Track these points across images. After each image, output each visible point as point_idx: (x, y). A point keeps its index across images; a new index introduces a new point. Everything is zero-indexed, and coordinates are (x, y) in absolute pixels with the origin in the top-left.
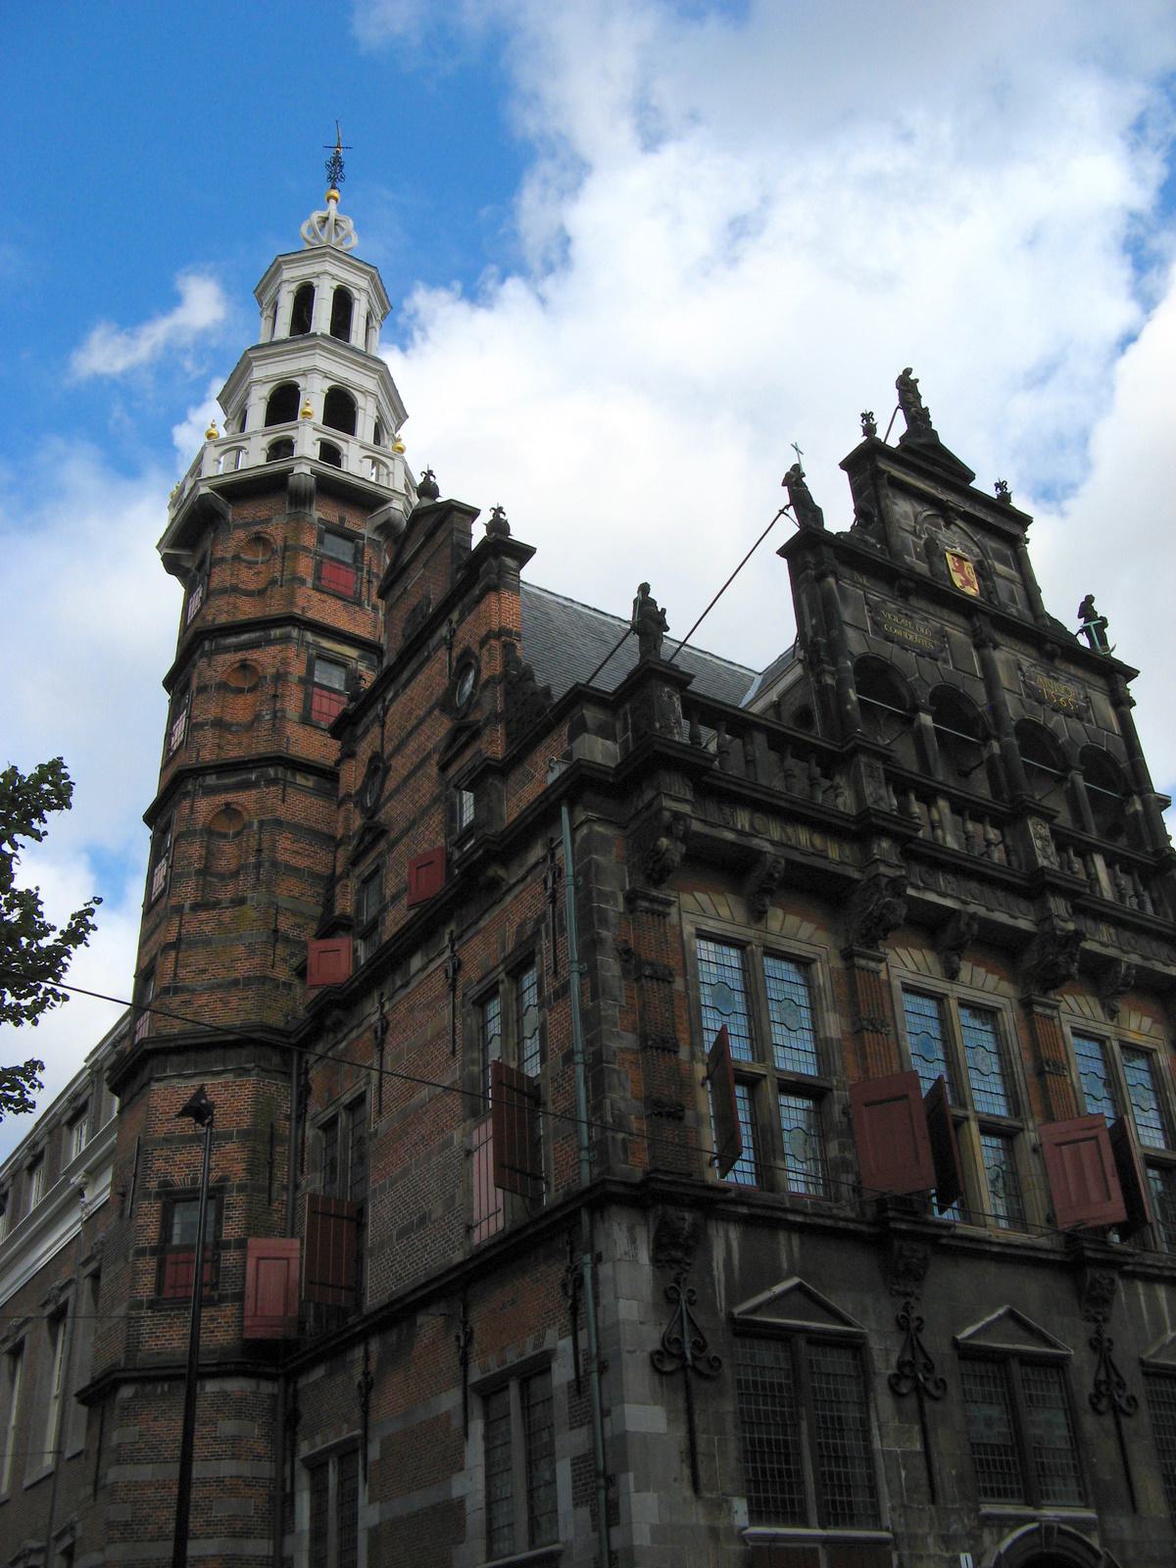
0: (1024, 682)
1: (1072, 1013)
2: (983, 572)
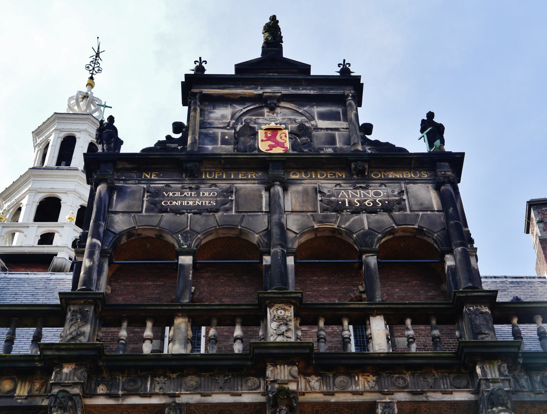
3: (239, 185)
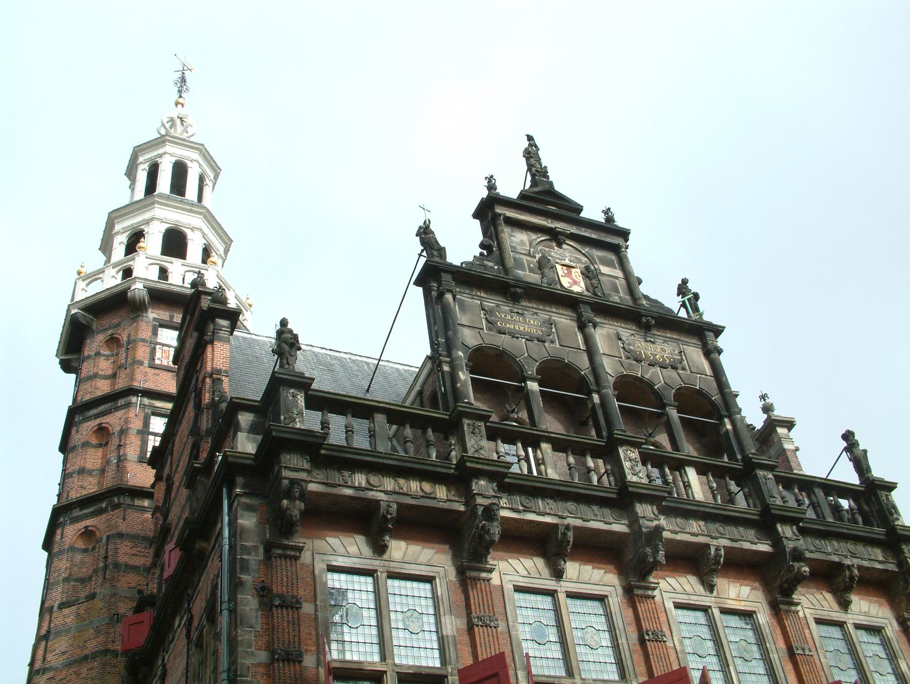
0: (624, 348)
1: (675, 591)
2: (588, 274)
3: (555, 318)
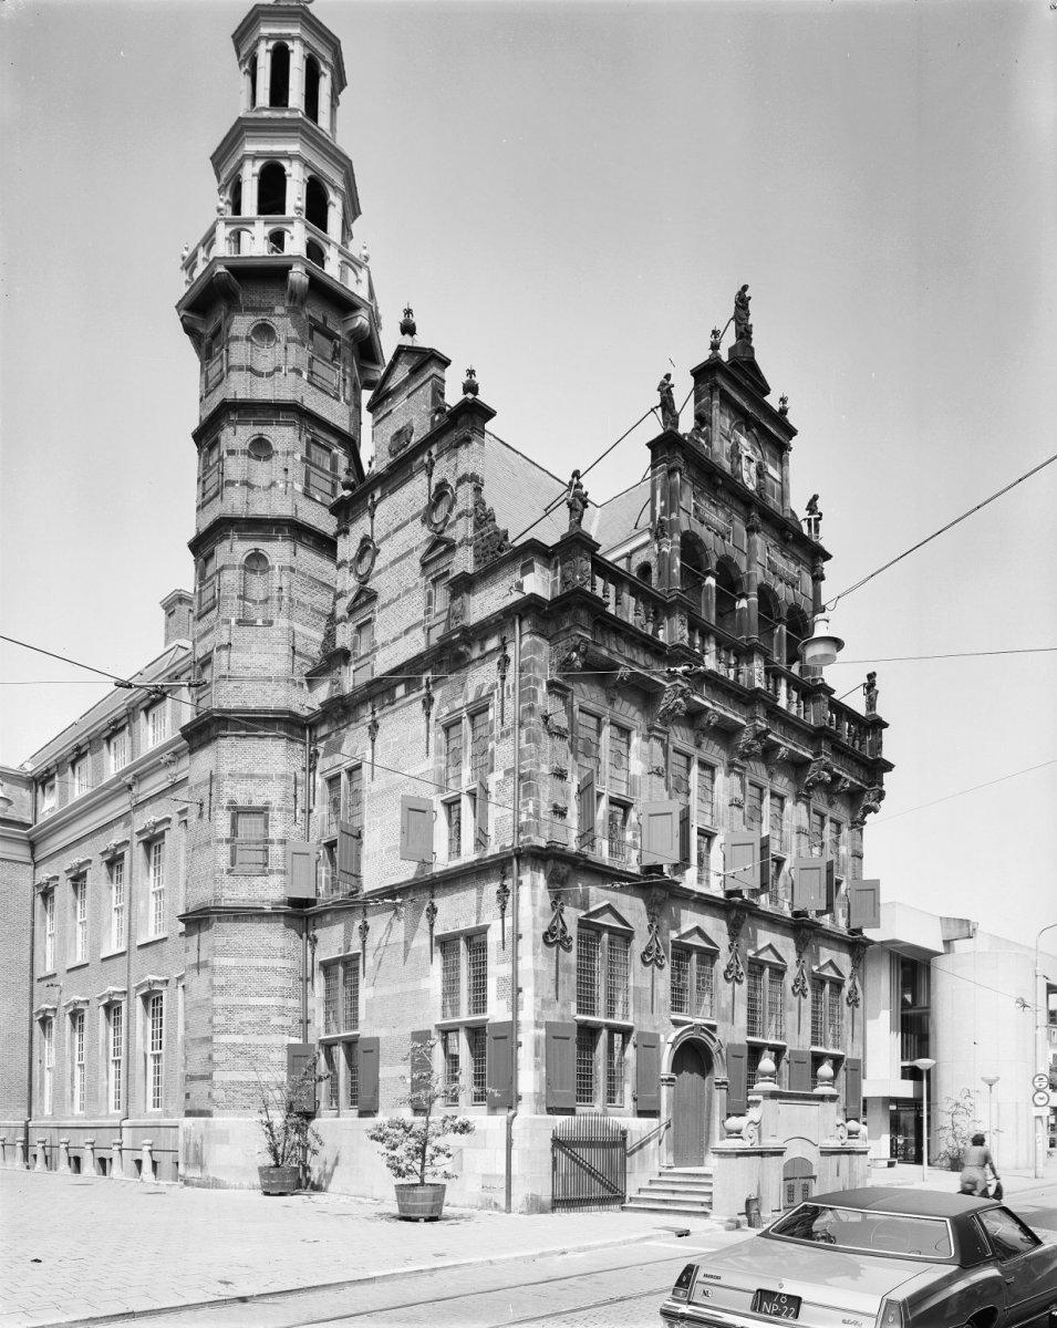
2: (761, 472)
